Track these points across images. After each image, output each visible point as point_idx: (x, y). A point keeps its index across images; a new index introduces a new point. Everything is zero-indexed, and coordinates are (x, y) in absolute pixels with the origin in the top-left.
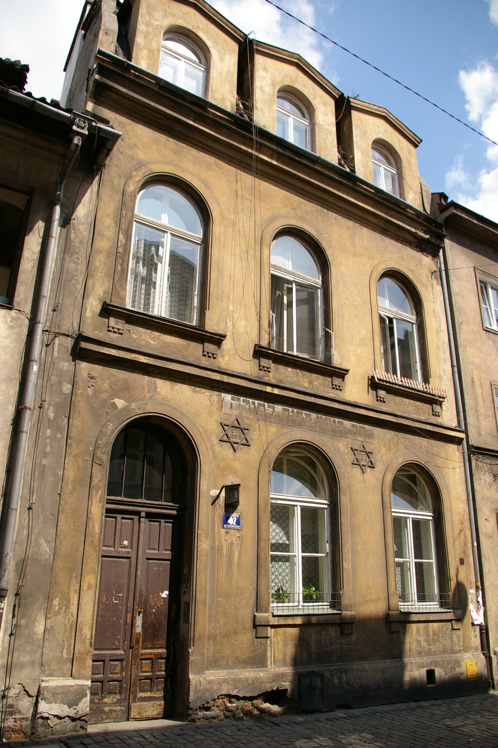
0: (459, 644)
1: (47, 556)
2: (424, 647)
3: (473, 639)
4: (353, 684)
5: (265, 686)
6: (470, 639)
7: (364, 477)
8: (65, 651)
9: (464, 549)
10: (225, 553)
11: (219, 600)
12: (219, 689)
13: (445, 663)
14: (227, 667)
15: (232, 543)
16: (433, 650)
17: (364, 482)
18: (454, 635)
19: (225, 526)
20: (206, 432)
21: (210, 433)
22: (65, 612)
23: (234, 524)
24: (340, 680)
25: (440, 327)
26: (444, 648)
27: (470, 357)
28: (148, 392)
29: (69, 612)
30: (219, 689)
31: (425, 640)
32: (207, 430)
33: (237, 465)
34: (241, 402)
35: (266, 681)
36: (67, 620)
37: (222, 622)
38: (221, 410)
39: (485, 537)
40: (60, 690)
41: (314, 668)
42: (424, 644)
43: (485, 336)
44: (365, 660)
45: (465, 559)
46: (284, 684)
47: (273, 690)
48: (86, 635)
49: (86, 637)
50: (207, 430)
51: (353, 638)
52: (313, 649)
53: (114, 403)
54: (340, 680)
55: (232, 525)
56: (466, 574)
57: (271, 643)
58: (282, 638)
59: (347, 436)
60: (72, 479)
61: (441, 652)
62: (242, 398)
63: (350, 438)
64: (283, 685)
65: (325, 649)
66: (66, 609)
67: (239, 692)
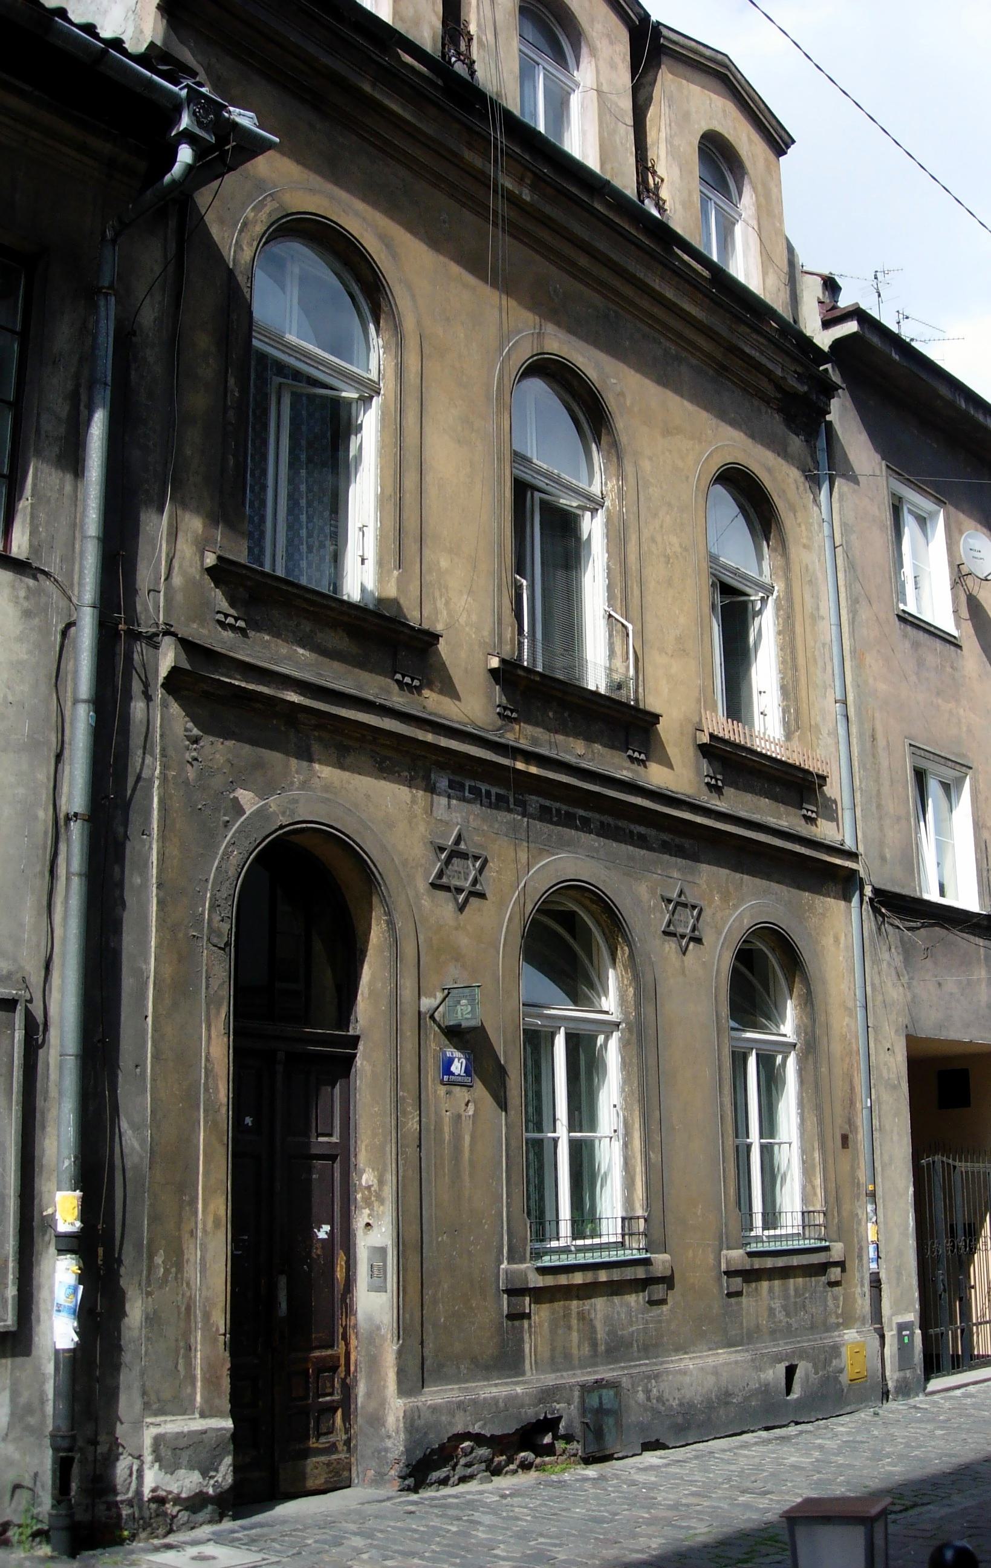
0: (836, 1312)
1: (136, 1159)
2: (780, 1321)
3: (859, 1301)
4: (668, 1400)
5: (526, 1413)
6: (855, 1301)
7: (683, 961)
8: (181, 1361)
10: (447, 1138)
11: (440, 1239)
12: (450, 1423)
14: (457, 1379)
15: (459, 1116)
16: (795, 1326)
17: (683, 973)
18: (830, 1294)
19: (446, 1078)
20: (405, 863)
21: (412, 867)
22: (176, 1278)
23: (462, 1074)
24: (647, 1392)
25: (818, 609)
26: (812, 1323)
27: (871, 681)
28: (297, 773)
29: (182, 1279)
30: (450, 1423)
31: (782, 1306)
32: (406, 859)
33: (464, 941)
34: (467, 794)
35: (527, 1402)
36: (180, 1296)
37: (446, 1286)
38: (431, 812)
39: (886, 1088)
40: (183, 1443)
41: (606, 1373)
42: (781, 1316)
43: (899, 631)
44: (686, 1353)
45: (850, 1136)
46: (558, 1406)
47: (539, 1420)
48: (217, 1325)
49: (217, 1329)
50: (406, 859)
52: (601, 1334)
53: (236, 799)
54: (647, 1392)
55: (459, 1075)
57: (530, 1326)
58: (547, 1314)
59: (653, 870)
60: (169, 981)
61: (807, 1329)
62: (468, 783)
63: (659, 872)
64: (555, 1409)
65: (620, 1333)
66: (176, 1274)
67: (483, 1427)
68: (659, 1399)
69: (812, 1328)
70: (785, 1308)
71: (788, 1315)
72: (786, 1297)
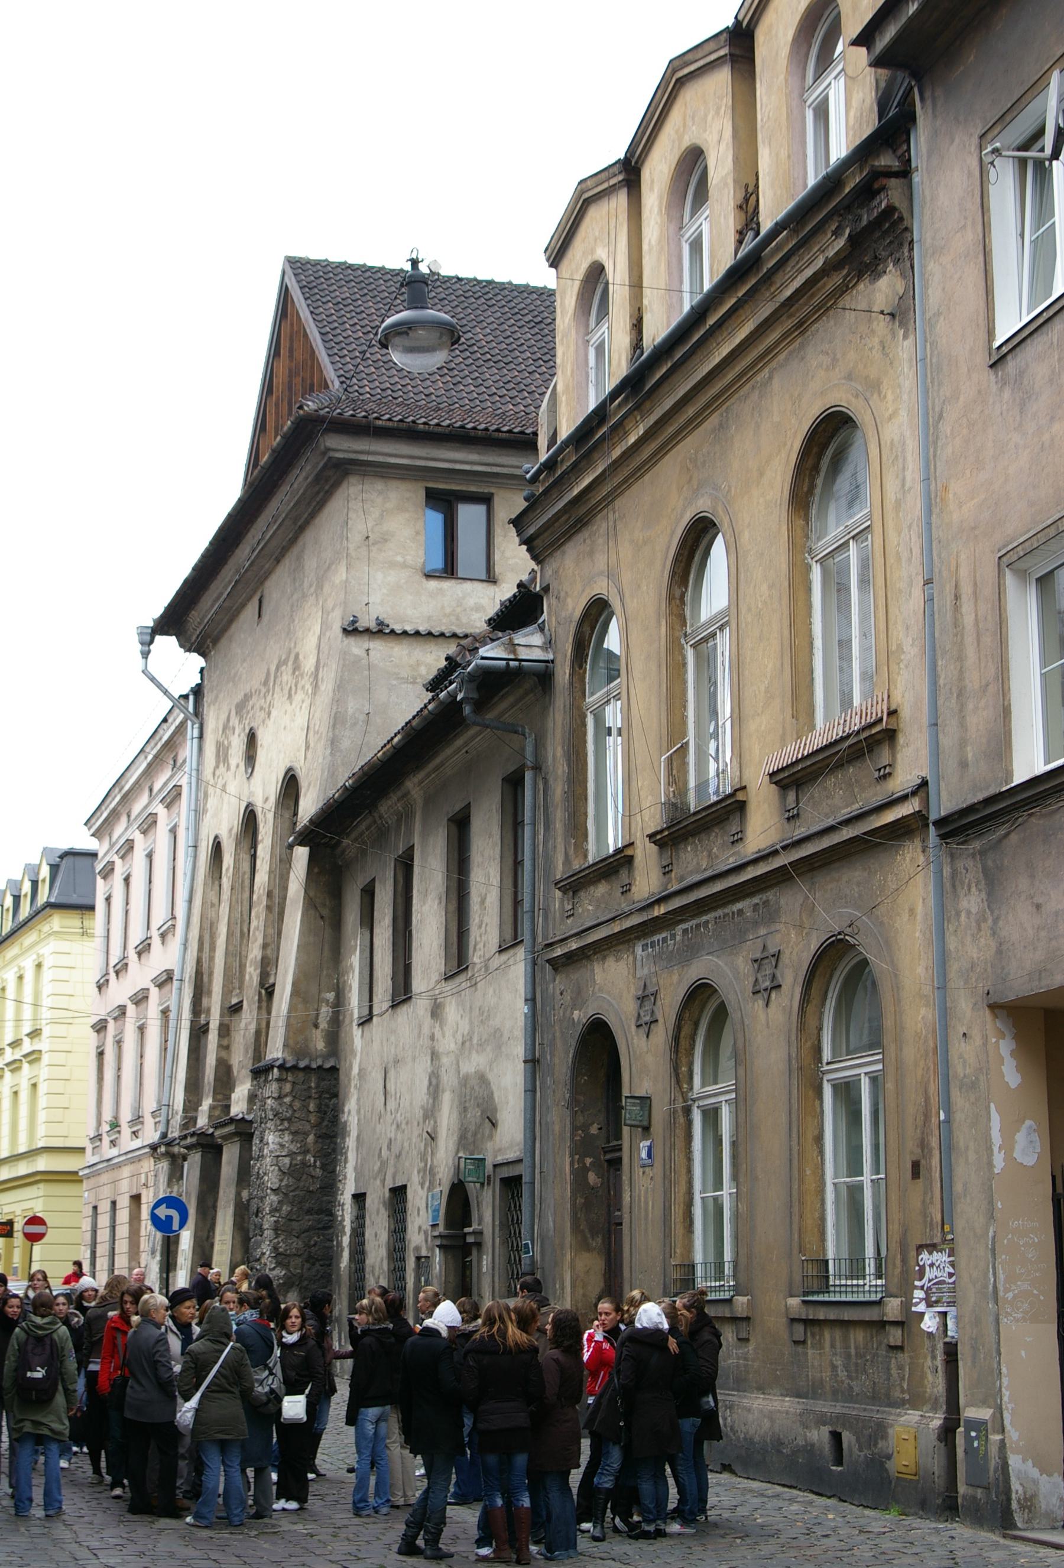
2: (842, 1382)
3: (930, 1377)
6: (923, 1376)
9: (923, 1133)
13: (860, 1424)
16: (856, 1390)
17: (768, 1026)
18: (893, 1361)
39: (960, 1089)
42: (842, 1374)
44: (763, 1393)
45: (923, 1162)
51: (751, 1346)
56: (924, 1202)
61: (868, 1397)
68: (732, 1428)
69: (873, 1398)
70: (846, 1367)
71: (849, 1377)
72: (848, 1356)
